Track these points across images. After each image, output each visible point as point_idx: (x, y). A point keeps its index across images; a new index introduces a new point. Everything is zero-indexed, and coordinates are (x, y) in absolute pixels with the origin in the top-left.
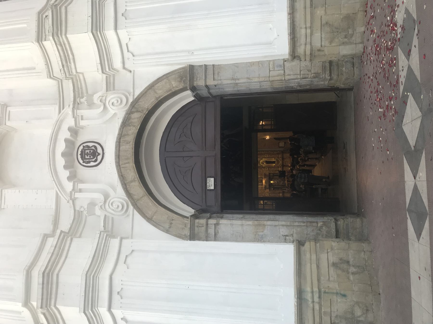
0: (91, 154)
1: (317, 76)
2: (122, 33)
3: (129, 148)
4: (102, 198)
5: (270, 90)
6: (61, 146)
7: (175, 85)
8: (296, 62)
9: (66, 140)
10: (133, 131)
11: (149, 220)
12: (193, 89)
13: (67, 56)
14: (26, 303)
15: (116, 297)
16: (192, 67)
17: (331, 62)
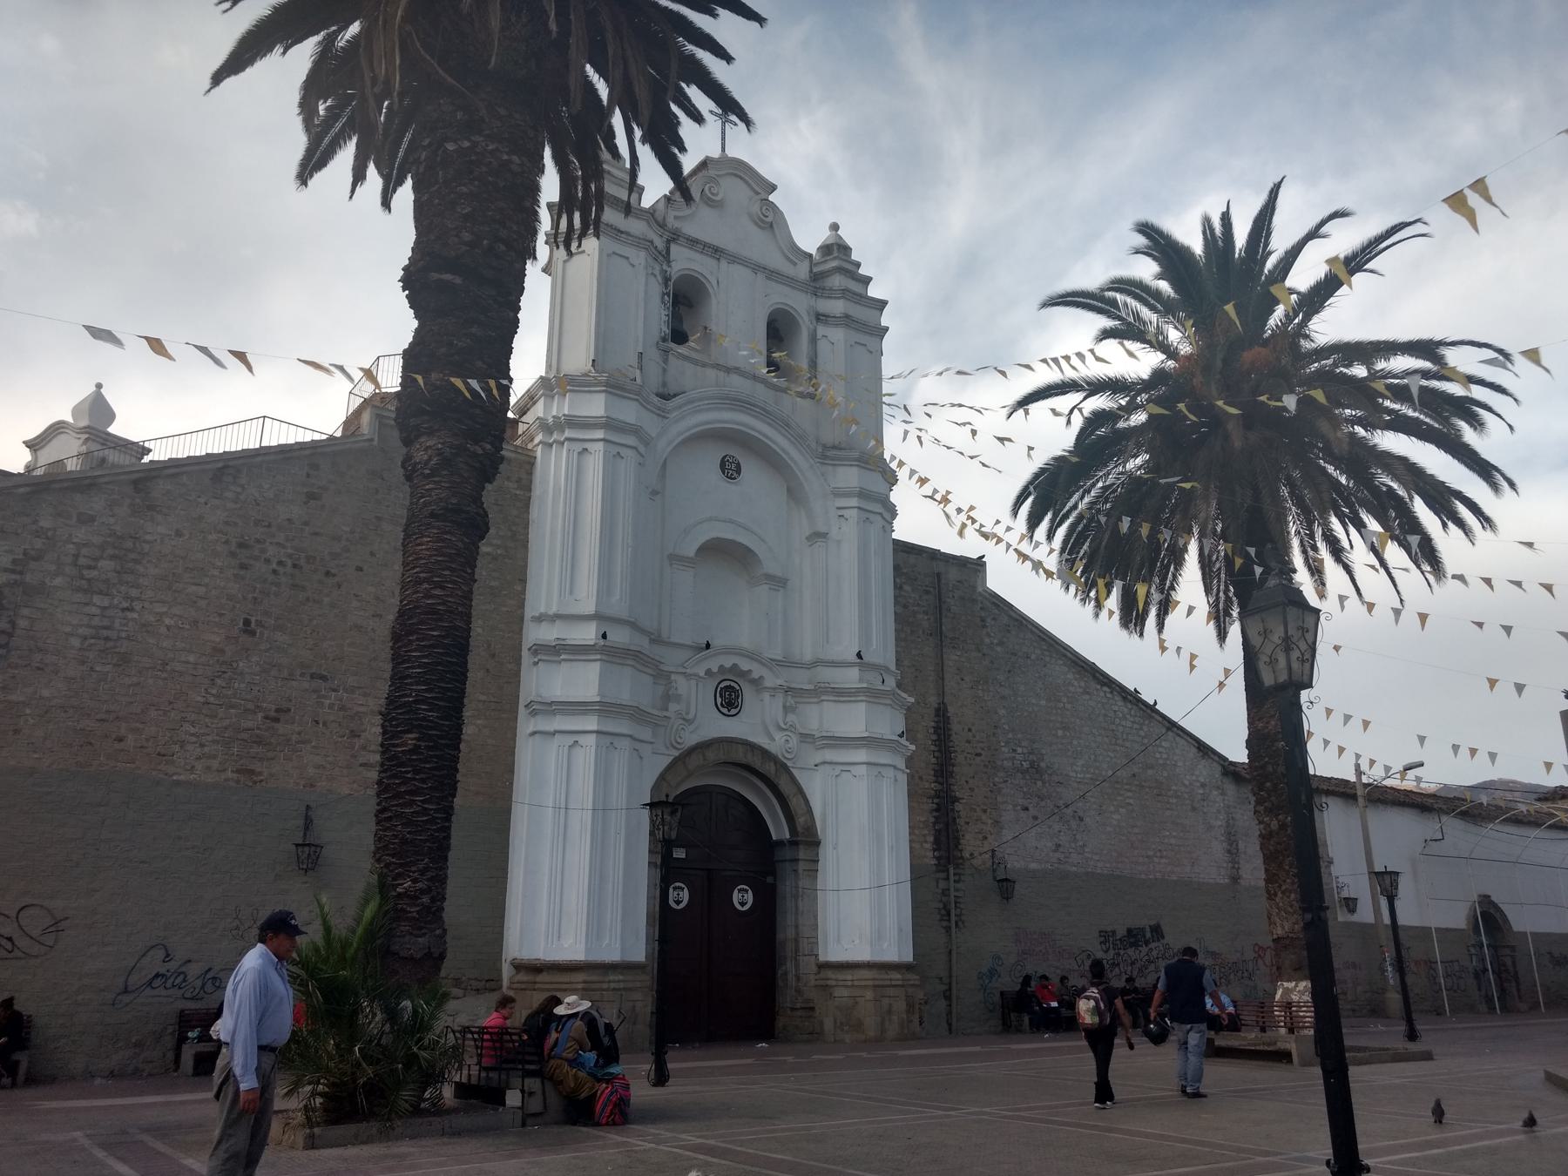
0: (729, 700)
1: (798, 991)
2: (863, 770)
3: (740, 755)
4: (690, 716)
5: (780, 936)
6: (745, 665)
7: (801, 821)
8: (815, 969)
9: (750, 671)
10: (757, 763)
11: (662, 777)
12: (794, 843)
13: (842, 694)
14: (597, 617)
15: (608, 739)
16: (817, 844)
17: (812, 1009)
